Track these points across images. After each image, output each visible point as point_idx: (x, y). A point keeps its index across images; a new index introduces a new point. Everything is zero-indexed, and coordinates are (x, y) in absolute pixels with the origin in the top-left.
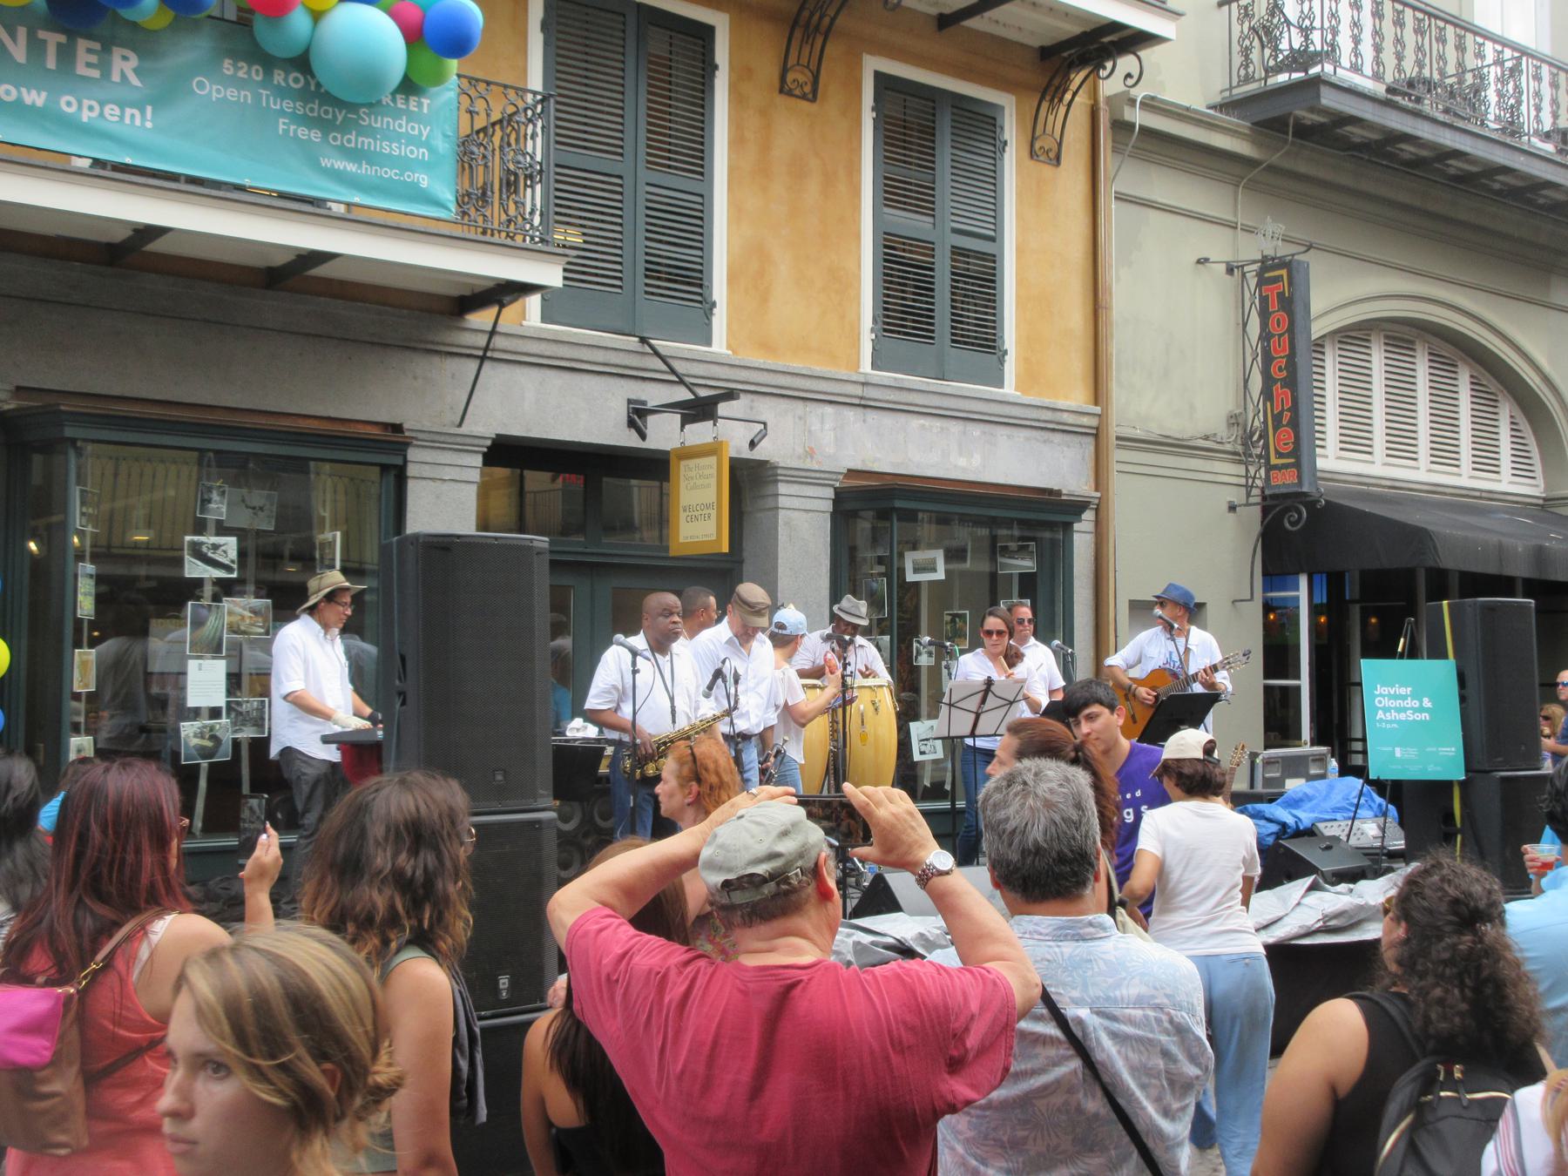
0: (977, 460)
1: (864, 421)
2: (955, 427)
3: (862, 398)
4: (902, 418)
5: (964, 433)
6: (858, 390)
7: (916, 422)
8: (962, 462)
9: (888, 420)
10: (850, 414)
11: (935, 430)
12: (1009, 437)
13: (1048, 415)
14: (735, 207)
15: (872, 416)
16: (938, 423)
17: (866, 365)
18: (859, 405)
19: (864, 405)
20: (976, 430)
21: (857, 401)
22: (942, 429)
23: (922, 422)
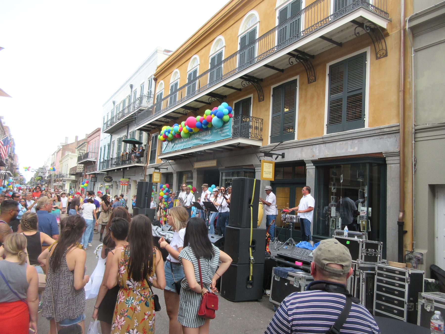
0: (356, 149)
1: (325, 146)
2: (349, 142)
3: (323, 141)
4: (335, 143)
5: (352, 143)
6: (322, 140)
7: (338, 143)
8: (352, 150)
9: (331, 145)
10: (322, 145)
11: (344, 144)
12: (367, 140)
13: (379, 131)
14: (300, 111)
15: (327, 145)
16: (344, 142)
17: (325, 134)
18: (323, 143)
19: (324, 143)
20: (356, 141)
21: (322, 142)
22: (346, 143)
23: (340, 143)
